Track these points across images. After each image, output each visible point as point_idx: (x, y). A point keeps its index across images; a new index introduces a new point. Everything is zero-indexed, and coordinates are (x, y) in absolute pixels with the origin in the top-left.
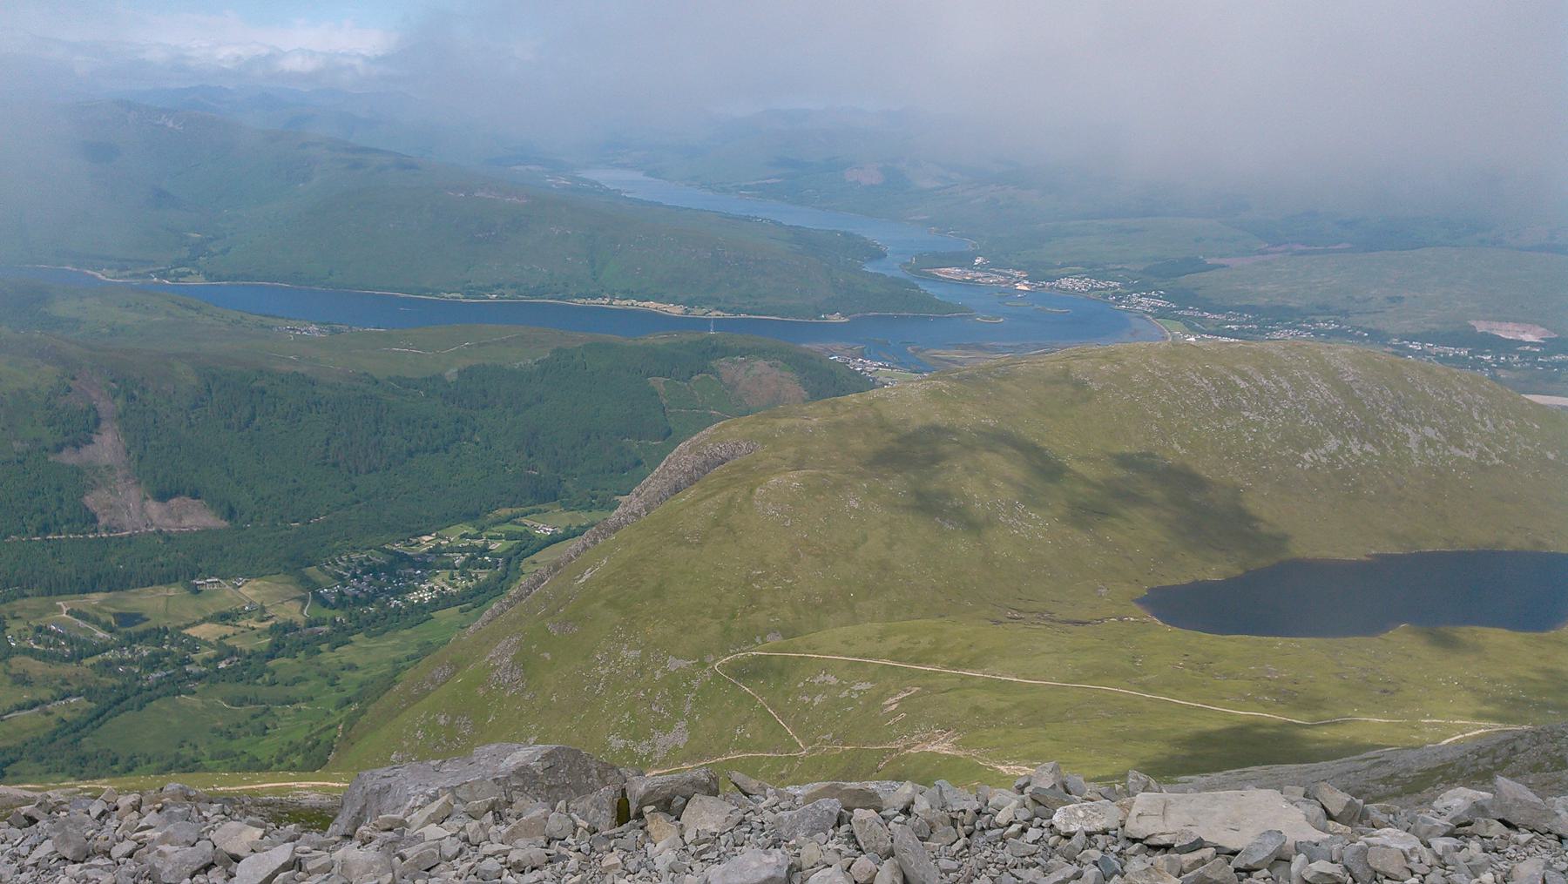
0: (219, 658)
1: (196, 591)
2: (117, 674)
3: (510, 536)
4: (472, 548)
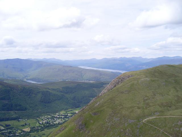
0: (21, 132)
1: (19, 121)
2: (4, 135)
3: (71, 113)
4: (64, 115)
